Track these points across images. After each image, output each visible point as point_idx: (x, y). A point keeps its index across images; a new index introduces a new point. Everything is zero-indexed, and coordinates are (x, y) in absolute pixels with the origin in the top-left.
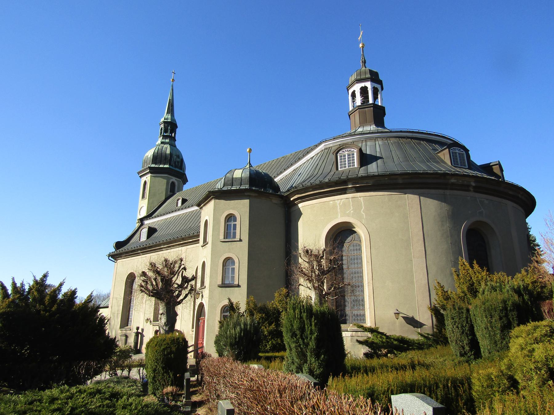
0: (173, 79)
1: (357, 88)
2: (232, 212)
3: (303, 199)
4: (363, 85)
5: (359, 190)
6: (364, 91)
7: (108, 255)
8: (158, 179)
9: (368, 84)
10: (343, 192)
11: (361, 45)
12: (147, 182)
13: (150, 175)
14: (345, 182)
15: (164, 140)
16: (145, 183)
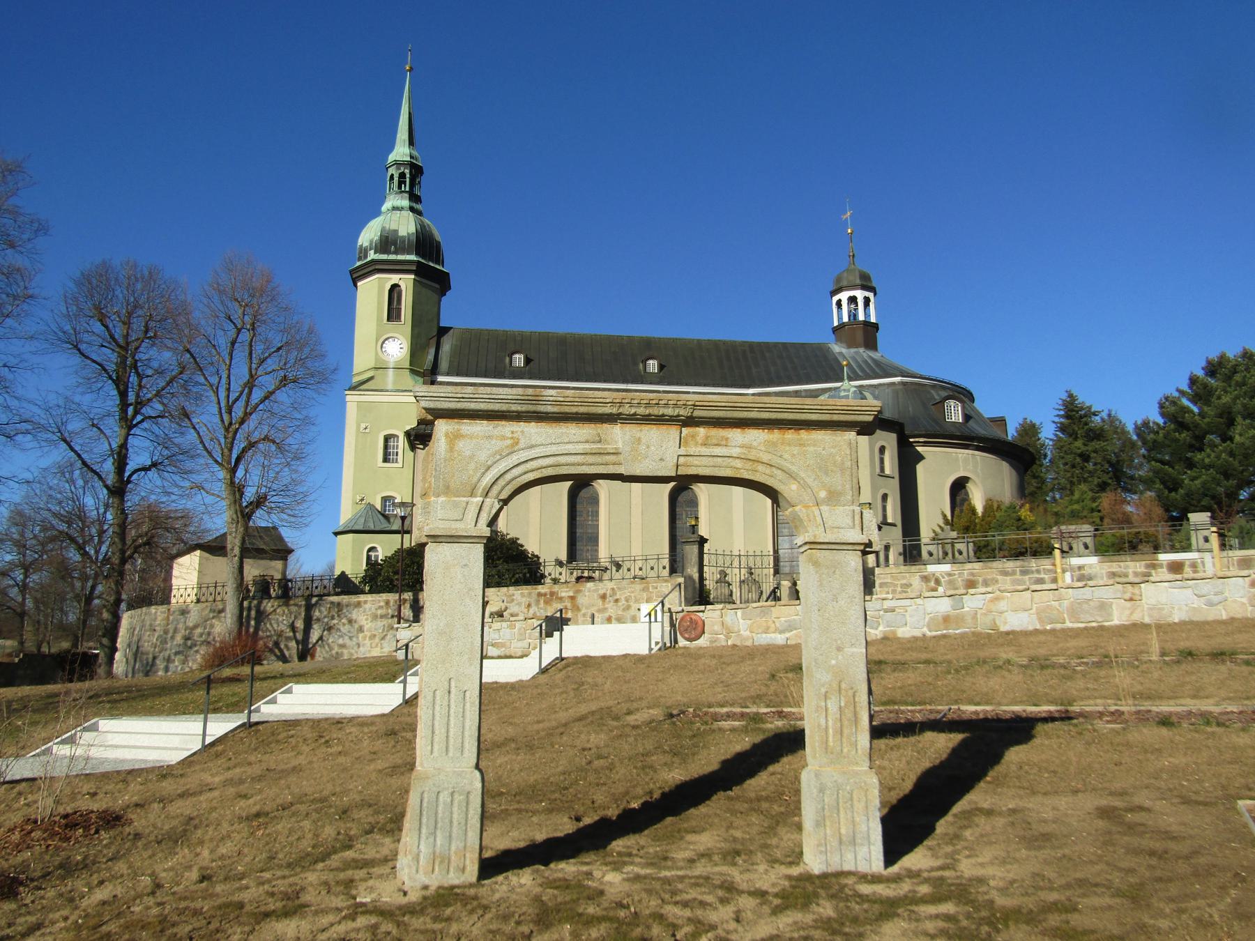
0: (411, 69)
1: (860, 294)
2: (884, 444)
3: (925, 444)
4: (867, 294)
5: (978, 449)
6: (867, 301)
7: (413, 433)
8: (424, 291)
9: (871, 295)
11: (849, 231)
12: (403, 287)
13: (413, 276)
14: (972, 439)
15: (414, 205)
16: (395, 288)
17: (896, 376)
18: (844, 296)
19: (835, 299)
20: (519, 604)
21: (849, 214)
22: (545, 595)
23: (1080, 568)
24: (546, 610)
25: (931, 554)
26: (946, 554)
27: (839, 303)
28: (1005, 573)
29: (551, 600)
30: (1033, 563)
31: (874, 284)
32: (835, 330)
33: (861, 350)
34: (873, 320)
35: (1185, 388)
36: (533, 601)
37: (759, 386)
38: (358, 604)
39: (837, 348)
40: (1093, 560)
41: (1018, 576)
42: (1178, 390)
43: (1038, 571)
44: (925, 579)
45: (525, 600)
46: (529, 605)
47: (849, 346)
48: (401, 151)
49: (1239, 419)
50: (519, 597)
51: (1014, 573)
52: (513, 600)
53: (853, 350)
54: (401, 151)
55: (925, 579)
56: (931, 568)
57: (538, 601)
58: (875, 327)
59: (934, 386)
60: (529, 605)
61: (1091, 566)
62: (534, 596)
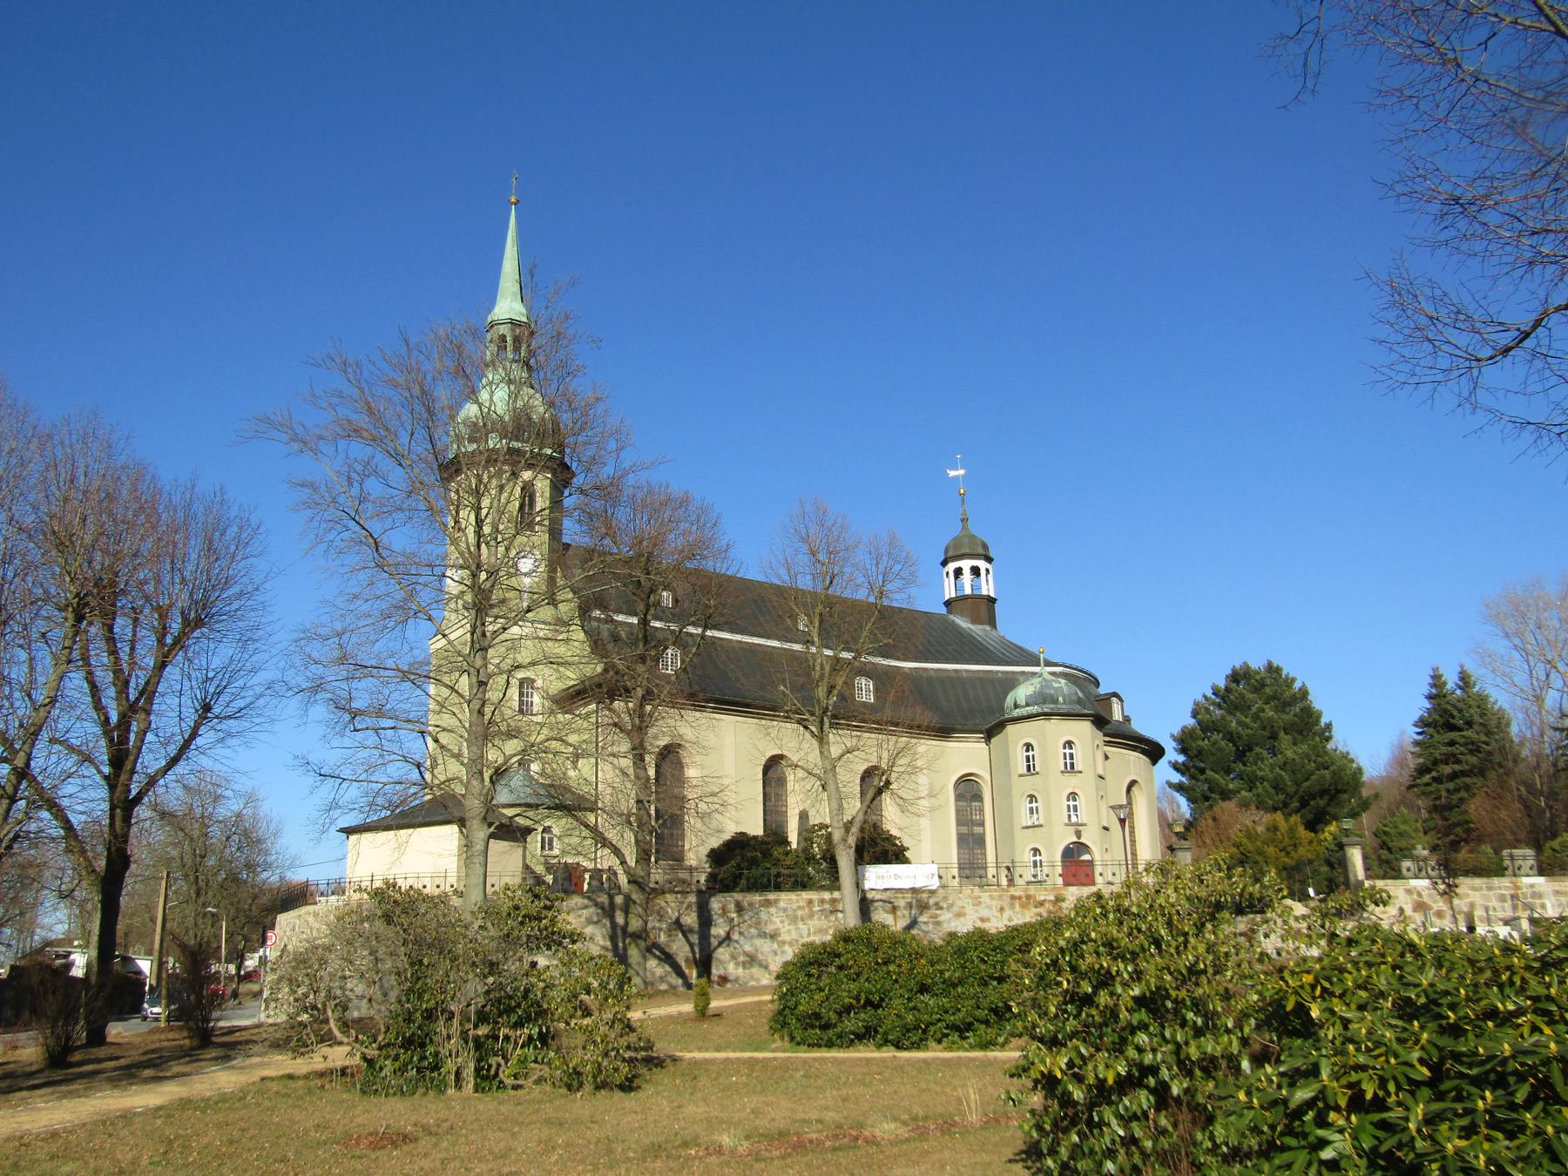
1: (982, 564)
10: (1134, 748)
17: (1057, 665)
18: (966, 565)
19: (952, 566)
20: (990, 908)
21: (962, 472)
22: (1020, 898)
23: (1532, 886)
24: (1023, 915)
25: (1408, 870)
26: (1420, 870)
27: (958, 572)
28: (1474, 889)
29: (1028, 904)
30: (1496, 881)
31: (991, 555)
32: (948, 603)
33: (988, 628)
34: (992, 595)
35: (1209, 694)
36: (1005, 904)
37: (916, 661)
38: (768, 903)
39: (963, 623)
40: (1541, 880)
41: (1485, 892)
42: (1205, 697)
43: (1500, 888)
44: (1409, 892)
45: (996, 904)
46: (1002, 909)
47: (974, 622)
48: (508, 306)
49: (1282, 734)
50: (988, 900)
51: (1481, 889)
52: (980, 903)
53: (980, 627)
54: (508, 306)
55: (1409, 892)
56: (1414, 883)
57: (1012, 906)
58: (991, 601)
59: (1085, 679)
60: (1002, 909)
61: (1540, 885)
62: (1007, 900)
